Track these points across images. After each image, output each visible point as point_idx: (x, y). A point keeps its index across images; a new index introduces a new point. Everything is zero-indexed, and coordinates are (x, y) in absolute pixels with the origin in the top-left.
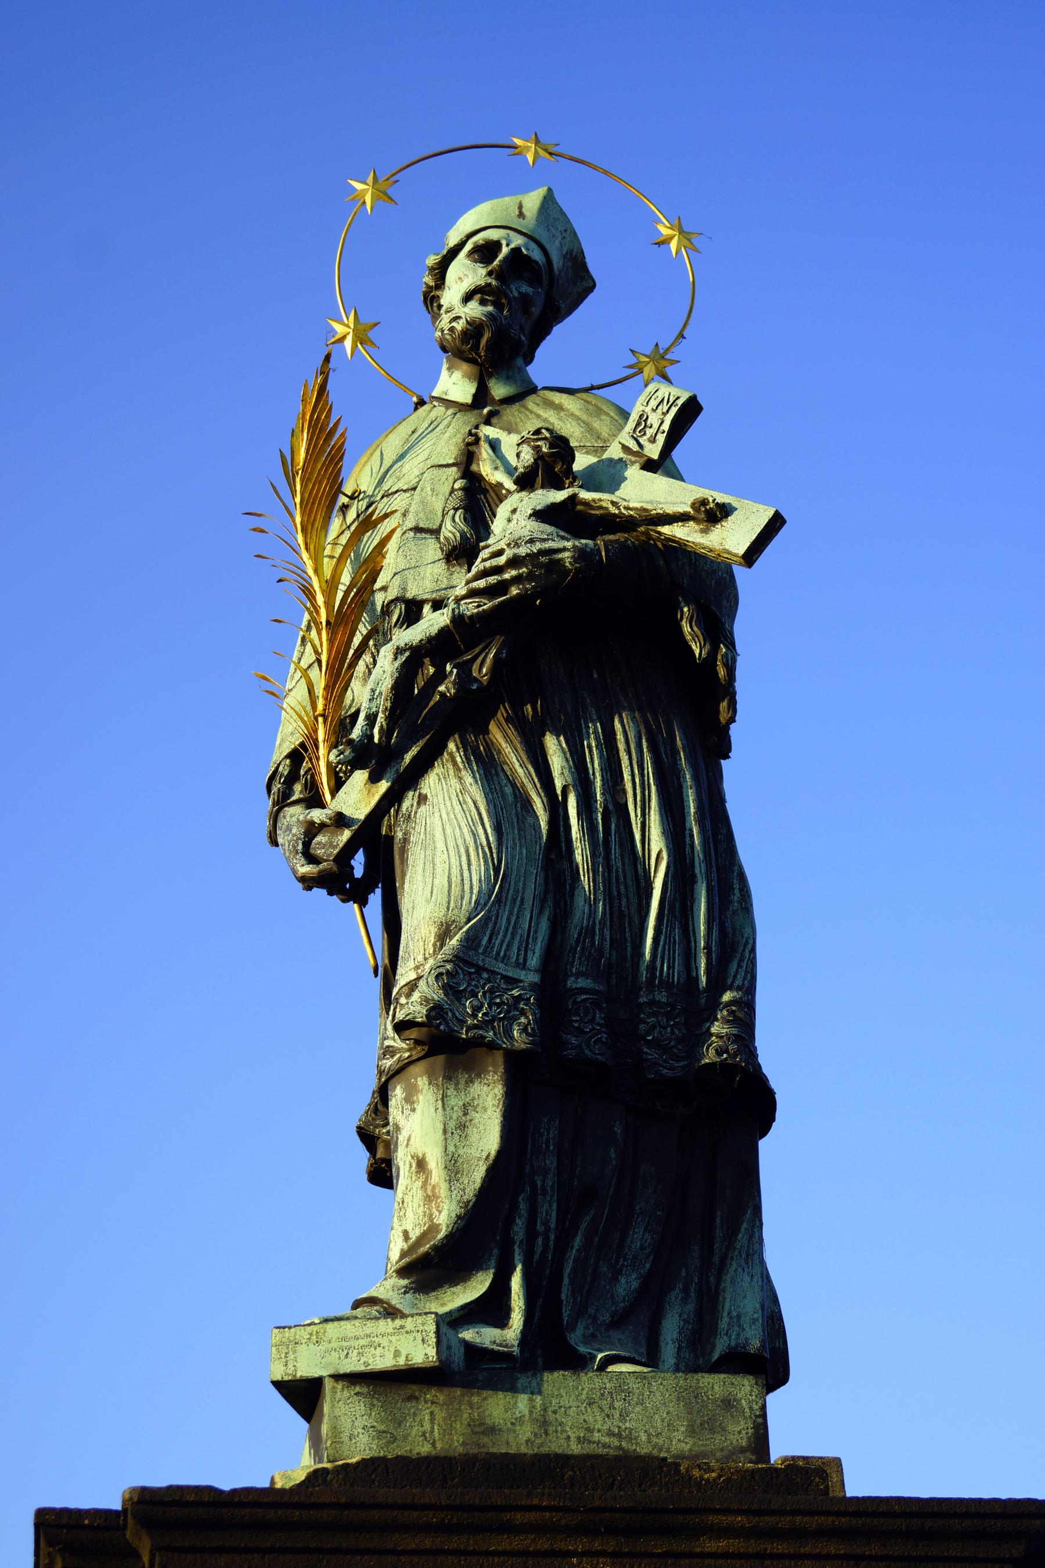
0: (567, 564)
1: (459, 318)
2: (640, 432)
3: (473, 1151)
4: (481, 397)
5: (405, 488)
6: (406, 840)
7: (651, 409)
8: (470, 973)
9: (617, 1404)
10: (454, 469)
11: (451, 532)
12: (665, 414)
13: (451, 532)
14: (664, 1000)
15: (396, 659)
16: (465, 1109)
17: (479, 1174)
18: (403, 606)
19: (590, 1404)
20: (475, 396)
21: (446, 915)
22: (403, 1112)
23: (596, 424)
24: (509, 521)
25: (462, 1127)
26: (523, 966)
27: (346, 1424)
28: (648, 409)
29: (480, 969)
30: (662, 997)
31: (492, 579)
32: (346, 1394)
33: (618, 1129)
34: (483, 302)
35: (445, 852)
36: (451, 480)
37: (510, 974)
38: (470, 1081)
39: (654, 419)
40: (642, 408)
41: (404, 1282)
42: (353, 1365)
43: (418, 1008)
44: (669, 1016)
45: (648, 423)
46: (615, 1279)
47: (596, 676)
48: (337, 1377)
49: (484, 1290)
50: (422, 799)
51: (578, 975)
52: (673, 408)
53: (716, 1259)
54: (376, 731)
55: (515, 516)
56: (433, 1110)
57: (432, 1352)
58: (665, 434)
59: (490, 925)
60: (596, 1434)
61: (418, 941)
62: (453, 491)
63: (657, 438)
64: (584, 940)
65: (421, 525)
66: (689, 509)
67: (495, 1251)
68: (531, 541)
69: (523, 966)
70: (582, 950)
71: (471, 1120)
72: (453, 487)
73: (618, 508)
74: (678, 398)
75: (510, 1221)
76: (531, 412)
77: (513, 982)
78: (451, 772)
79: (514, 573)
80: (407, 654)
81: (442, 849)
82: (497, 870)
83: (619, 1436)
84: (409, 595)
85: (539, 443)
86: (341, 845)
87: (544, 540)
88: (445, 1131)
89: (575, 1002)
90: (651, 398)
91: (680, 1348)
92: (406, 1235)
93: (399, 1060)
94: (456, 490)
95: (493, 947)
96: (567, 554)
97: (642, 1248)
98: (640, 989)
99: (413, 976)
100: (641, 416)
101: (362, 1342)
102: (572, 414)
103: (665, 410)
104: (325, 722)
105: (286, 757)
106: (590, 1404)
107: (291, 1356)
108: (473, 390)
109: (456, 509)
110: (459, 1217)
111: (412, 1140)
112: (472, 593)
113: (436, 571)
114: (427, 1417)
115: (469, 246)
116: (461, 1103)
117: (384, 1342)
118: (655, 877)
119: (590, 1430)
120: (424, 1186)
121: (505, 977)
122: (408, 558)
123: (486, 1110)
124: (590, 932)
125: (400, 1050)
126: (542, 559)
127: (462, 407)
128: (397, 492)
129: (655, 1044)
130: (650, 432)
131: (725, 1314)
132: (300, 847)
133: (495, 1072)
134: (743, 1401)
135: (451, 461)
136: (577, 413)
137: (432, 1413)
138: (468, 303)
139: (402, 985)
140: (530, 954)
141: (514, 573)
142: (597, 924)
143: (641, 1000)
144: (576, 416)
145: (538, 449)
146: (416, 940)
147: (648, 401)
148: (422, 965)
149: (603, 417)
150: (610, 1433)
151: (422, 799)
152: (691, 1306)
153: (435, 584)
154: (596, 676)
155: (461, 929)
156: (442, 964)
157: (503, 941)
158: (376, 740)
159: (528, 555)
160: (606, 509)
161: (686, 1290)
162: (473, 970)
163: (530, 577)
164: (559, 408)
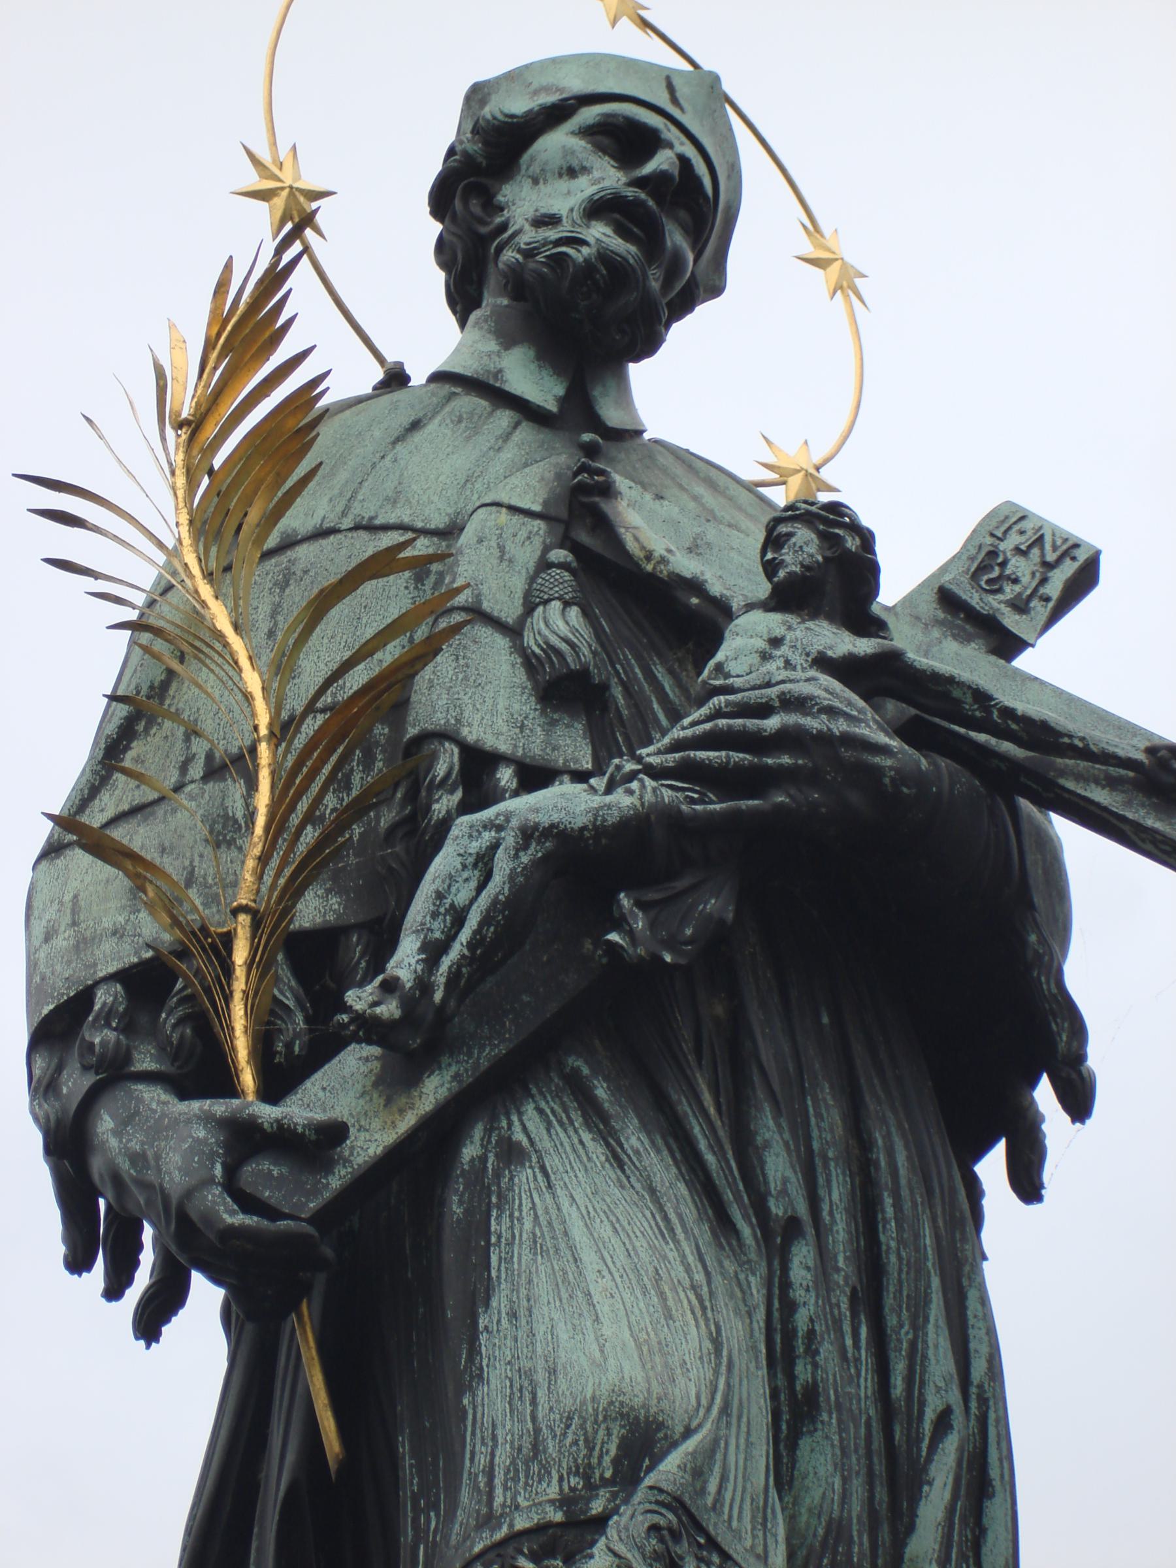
0: (887, 781)
1: (583, 242)
2: (989, 582)
7: (1012, 546)
8: (699, 1545)
12: (1048, 566)
15: (525, 847)
18: (456, 750)
20: (563, 401)
21: (645, 1406)
34: (622, 231)
35: (605, 1273)
36: (537, 543)
39: (1022, 567)
45: (1007, 572)
47: (825, 1020)
52: (1068, 561)
55: (777, 653)
58: (1051, 605)
59: (719, 1456)
61: (575, 1443)
62: (544, 565)
63: (1032, 605)
64: (835, 1552)
65: (486, 606)
66: (1140, 756)
73: (987, 710)
81: (597, 1267)
86: (327, 1195)
90: (1009, 528)
95: (722, 1505)
96: (889, 762)
100: (993, 554)
104: (256, 925)
105: (119, 976)
108: (560, 390)
109: (567, 604)
113: (516, 707)
115: (589, 114)
118: (929, 1459)
122: (462, 662)
126: (846, 754)
130: (1010, 591)
132: (218, 1170)
135: (537, 508)
138: (593, 223)
140: (770, 1541)
142: (855, 1521)
146: (568, 1441)
147: (1006, 532)
148: (581, 1497)
151: (512, 1154)
153: (517, 731)
154: (825, 1020)
155: (674, 1445)
156: (654, 1507)
157: (733, 1500)
160: (958, 702)
162: (702, 1541)
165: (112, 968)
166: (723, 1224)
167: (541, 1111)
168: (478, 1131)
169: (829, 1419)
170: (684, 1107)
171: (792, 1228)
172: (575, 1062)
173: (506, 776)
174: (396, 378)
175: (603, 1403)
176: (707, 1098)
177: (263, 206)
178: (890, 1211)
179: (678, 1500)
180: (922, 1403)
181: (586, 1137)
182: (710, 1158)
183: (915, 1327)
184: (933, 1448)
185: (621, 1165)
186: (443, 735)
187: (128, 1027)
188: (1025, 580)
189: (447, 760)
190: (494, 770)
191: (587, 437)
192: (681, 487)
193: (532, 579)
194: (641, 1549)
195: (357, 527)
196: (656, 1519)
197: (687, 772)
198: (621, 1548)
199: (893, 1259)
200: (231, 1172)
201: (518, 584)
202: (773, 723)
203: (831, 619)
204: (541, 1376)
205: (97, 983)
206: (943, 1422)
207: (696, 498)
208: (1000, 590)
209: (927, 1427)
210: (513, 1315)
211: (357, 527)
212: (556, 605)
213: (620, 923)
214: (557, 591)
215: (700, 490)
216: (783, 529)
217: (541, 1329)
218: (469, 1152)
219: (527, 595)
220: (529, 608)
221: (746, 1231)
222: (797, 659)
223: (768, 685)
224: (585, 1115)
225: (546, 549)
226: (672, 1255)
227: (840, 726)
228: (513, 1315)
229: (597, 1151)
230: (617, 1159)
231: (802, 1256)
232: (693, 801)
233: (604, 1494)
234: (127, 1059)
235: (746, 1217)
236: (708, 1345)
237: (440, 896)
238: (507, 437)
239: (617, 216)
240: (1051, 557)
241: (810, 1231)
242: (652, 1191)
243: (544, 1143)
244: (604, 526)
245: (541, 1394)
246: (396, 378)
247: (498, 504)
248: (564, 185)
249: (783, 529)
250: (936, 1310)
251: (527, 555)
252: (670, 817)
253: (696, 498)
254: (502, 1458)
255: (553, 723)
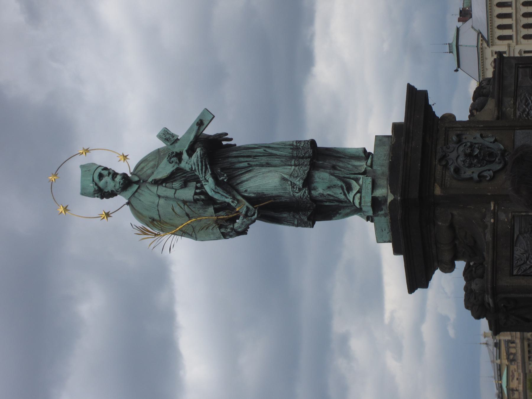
2: (169, 140)
3: (328, 178)
4: (137, 182)
5: (158, 200)
6: (254, 193)
9: (379, 155)
10: (159, 187)
11: (179, 185)
12: (168, 133)
13: (179, 185)
14: (296, 152)
16: (319, 178)
17: (332, 177)
19: (379, 159)
21: (280, 178)
22: (317, 191)
23: (151, 160)
24: (189, 164)
25: (323, 179)
26: (290, 169)
27: (380, 193)
28: (164, 137)
29: (292, 173)
30: (295, 152)
31: (204, 167)
32: (375, 193)
33: (321, 162)
34: (116, 177)
36: (162, 187)
37: (293, 170)
38: (314, 177)
39: (168, 136)
40: (163, 139)
41: (350, 192)
42: (370, 191)
43: (300, 181)
44: (299, 151)
46: (349, 168)
48: (372, 194)
49: (353, 180)
50: (246, 191)
51: (291, 162)
53: (344, 156)
54: (230, 197)
55: (188, 163)
56: (318, 184)
57: (370, 178)
60: (385, 158)
62: (166, 187)
65: (174, 193)
66: (198, 127)
67: (346, 179)
68: (198, 158)
69: (290, 169)
70: (285, 162)
71: (322, 178)
72: (164, 187)
74: (165, 130)
75: (340, 177)
76: (143, 173)
77: (294, 169)
78: (241, 184)
79: (203, 162)
80: (216, 186)
82: (269, 172)
83: (385, 156)
84: (193, 195)
85: (172, 156)
86: (252, 208)
87: (198, 155)
88: (324, 182)
89: (297, 163)
91: (361, 162)
92: (341, 193)
93: (307, 190)
94: (166, 186)
97: (343, 164)
98: (293, 156)
99: (290, 187)
101: (366, 189)
102: (146, 165)
103: (167, 133)
106: (379, 159)
107: (367, 202)
110: (340, 181)
111: (323, 189)
112: (205, 172)
114: (380, 182)
116: (318, 179)
117: (367, 186)
119: (384, 159)
120: (332, 187)
121: (294, 170)
123: (320, 175)
124: (282, 161)
125: (305, 191)
126: (202, 156)
127: (139, 188)
128: (158, 202)
129: (305, 154)
130: (171, 137)
131: (355, 154)
132: (250, 218)
133: (313, 173)
134: (380, 138)
135: (157, 187)
136: (146, 164)
137: (379, 181)
139: (291, 190)
141: (203, 162)
143: (296, 156)
144: (147, 164)
145: (173, 157)
149: (148, 159)
150: (385, 157)
152: (353, 161)
154: (220, 159)
155: (283, 176)
158: (231, 197)
159: (201, 159)
161: (349, 161)
163: (205, 160)
164: (143, 168)
165: (218, 230)
166: (250, 171)
167: (240, 188)
168: (243, 194)
169: (269, 162)
170: (237, 174)
171: (248, 164)
172: (235, 184)
173: (198, 191)
174: (128, 203)
175: (280, 182)
176: (234, 172)
177: (108, 218)
178: (243, 154)
179: (290, 176)
180: (262, 152)
181: (244, 183)
182: (243, 172)
183: (254, 153)
184: (267, 152)
185: (248, 180)
186: (193, 197)
187: (227, 228)
188: (170, 136)
189: (197, 197)
190: (197, 192)
191: (141, 181)
192: (145, 172)
193: (168, 188)
194: (296, 179)
195: (158, 207)
196: (293, 178)
197: (205, 172)
198: (296, 181)
199: (248, 154)
200: (249, 217)
201: (168, 189)
202: (200, 164)
203: (182, 157)
204: (275, 188)
205: (220, 231)
206: (265, 150)
207: (147, 170)
208: (171, 139)
209: (264, 152)
210: (267, 190)
211: (158, 207)
212: (173, 185)
213: (223, 180)
214: (171, 186)
215: (145, 170)
216: (171, 161)
217: (270, 188)
218: (246, 195)
219: (170, 188)
220: (173, 188)
221: (250, 169)
222: (189, 161)
223: (194, 164)
224: (241, 183)
225: (163, 186)
226: (259, 176)
227: (199, 157)
228: (267, 190)
229: (246, 183)
230: (247, 180)
231: (251, 163)
232: (209, 172)
233: (288, 182)
234: (231, 228)
235: (249, 168)
236: (270, 173)
237: (220, 197)
238: (143, 191)
239: (114, 178)
240: (167, 133)
241: (248, 162)
242: (251, 177)
243: (245, 187)
244: (160, 180)
245: (277, 188)
246: (128, 203)
247: (157, 192)
248: (108, 184)
249: (171, 161)
250: (252, 150)
251: (164, 189)
252: (211, 174)
253: (147, 170)
254: (283, 191)
255: (189, 186)
